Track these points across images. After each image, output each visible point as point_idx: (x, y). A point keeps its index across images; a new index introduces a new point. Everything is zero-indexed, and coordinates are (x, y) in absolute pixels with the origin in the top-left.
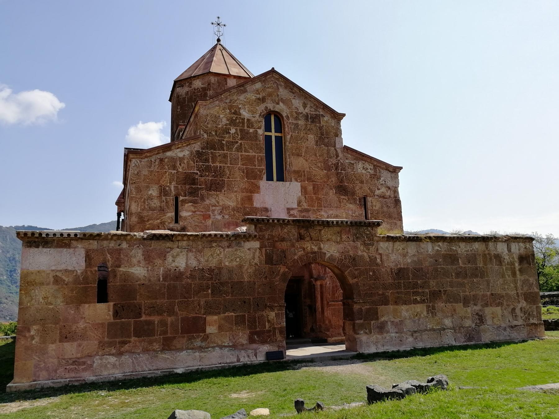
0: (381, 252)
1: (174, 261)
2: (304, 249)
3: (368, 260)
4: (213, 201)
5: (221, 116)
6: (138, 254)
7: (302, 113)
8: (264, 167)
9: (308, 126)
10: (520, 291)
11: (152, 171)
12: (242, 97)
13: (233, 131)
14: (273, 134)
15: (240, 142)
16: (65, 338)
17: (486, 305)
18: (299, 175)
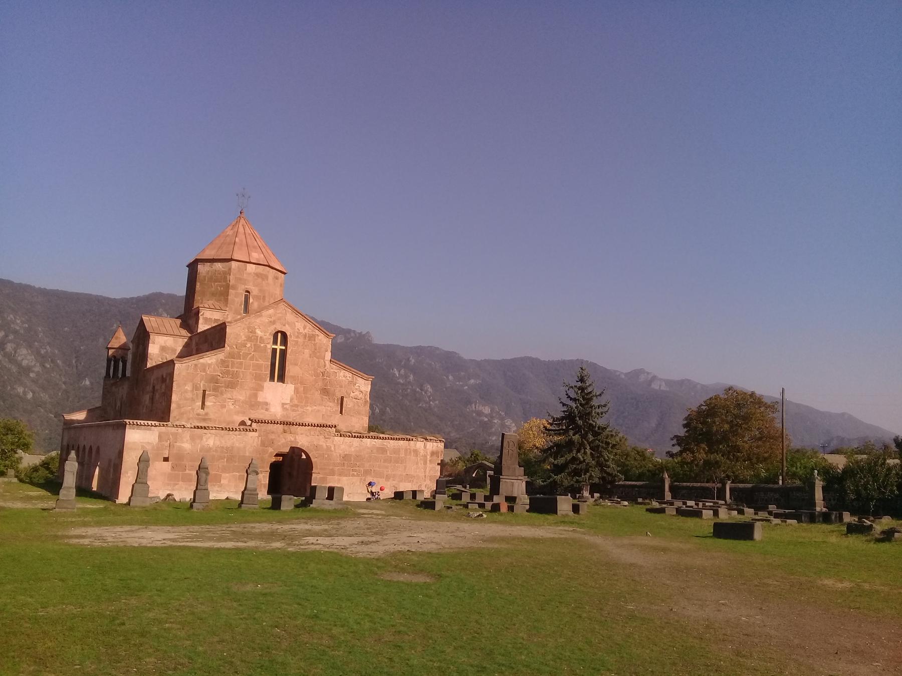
0: (334, 443)
1: (206, 441)
2: (285, 440)
3: (326, 448)
4: (229, 396)
5: (242, 334)
7: (302, 333)
9: (306, 343)
10: (427, 474)
11: (188, 373)
12: (258, 321)
13: (249, 345)
14: (279, 347)
15: (253, 353)
17: (401, 481)
18: (294, 379)
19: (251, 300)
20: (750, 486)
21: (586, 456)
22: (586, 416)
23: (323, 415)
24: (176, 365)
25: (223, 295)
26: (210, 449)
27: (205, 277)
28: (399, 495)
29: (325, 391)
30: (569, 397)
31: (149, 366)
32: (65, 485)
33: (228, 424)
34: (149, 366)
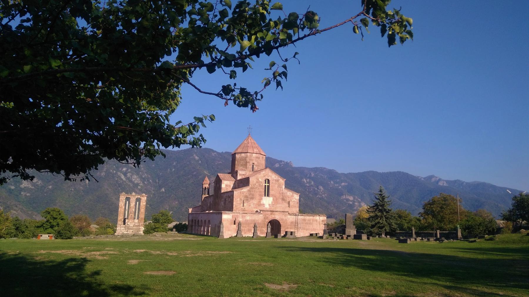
4: (251, 202)
6: (241, 216)
8: (264, 193)
12: (259, 176)
13: (257, 184)
14: (267, 185)
16: (229, 230)
18: (273, 196)
19: (255, 167)
20: (447, 232)
21: (383, 221)
22: (383, 206)
23: (283, 208)
24: (234, 192)
25: (245, 165)
26: (248, 220)
27: (238, 159)
28: (311, 235)
29: (283, 199)
30: (376, 198)
31: (222, 192)
32: (221, 231)
33: (252, 212)
34: (222, 192)
